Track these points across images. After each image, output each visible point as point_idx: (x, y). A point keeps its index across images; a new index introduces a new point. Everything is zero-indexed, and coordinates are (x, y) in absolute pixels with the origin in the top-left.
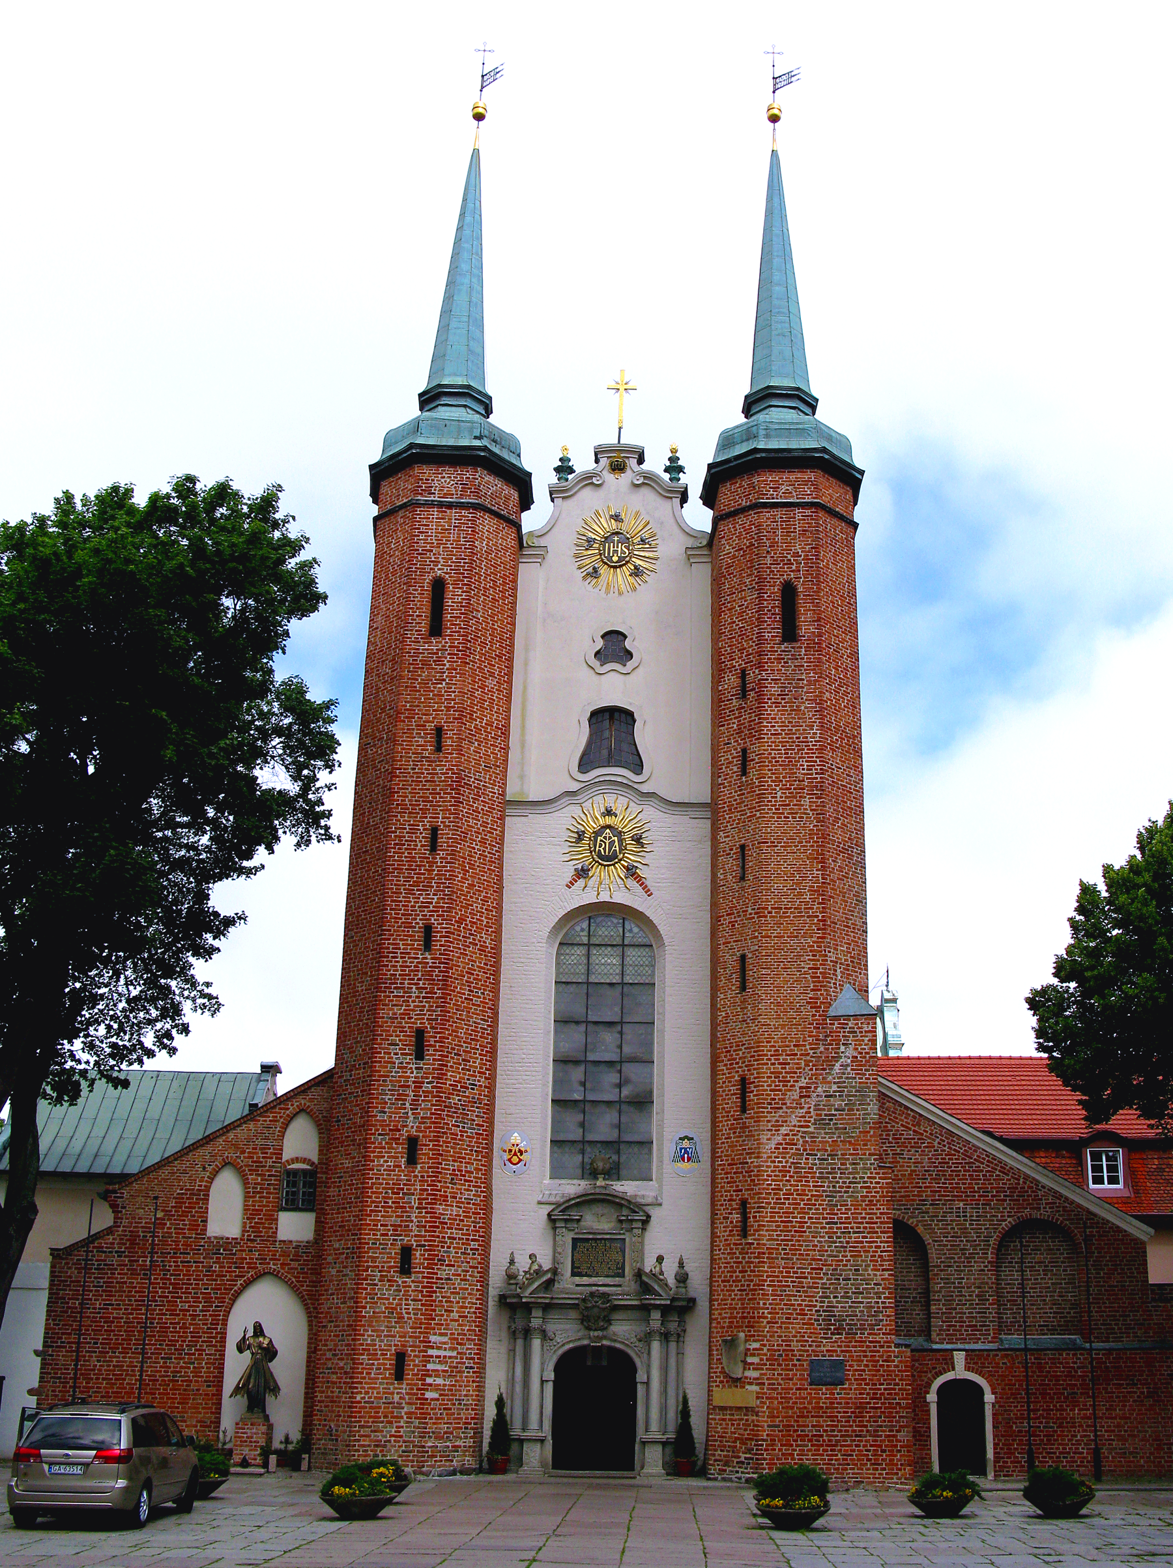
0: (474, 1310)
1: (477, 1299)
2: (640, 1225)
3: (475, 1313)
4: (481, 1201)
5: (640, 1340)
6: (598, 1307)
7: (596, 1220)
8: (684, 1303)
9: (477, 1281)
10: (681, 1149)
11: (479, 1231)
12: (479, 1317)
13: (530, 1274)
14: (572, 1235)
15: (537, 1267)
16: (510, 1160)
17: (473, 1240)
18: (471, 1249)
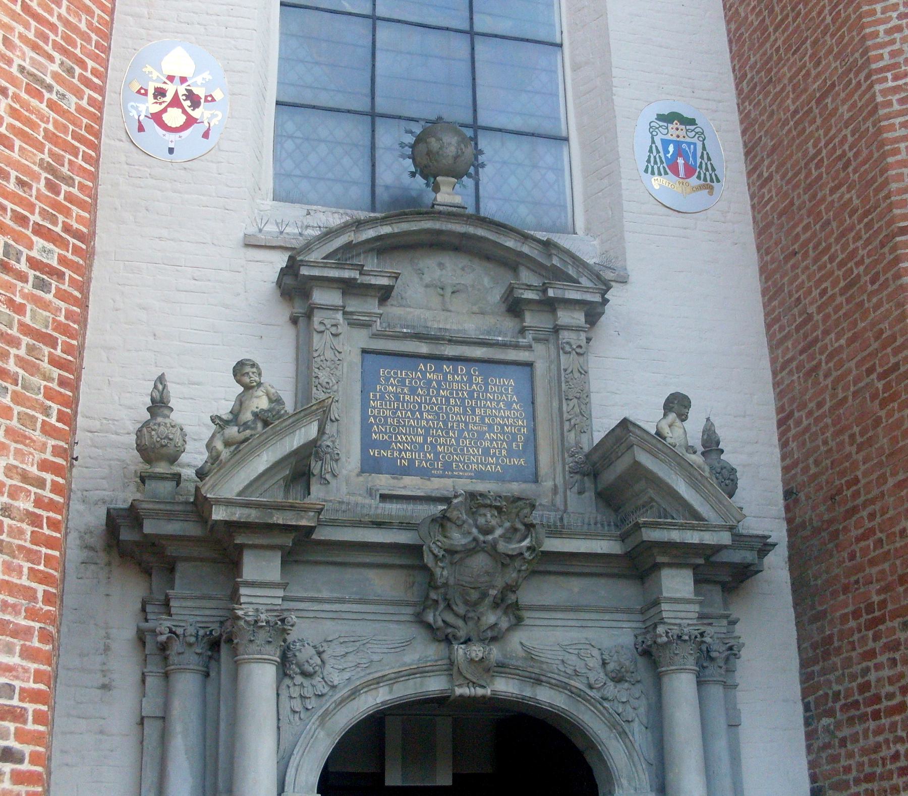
0: (30, 506)
1: (44, 466)
2: (578, 318)
3: (35, 520)
4: (79, 109)
5: (618, 679)
6: (492, 551)
7: (435, 301)
8: (748, 556)
9: (49, 394)
10: (666, 143)
11: (67, 212)
12: (50, 543)
13: (246, 426)
14: (361, 339)
15: (262, 403)
16: (157, 118)
17: (39, 230)
18: (33, 263)
